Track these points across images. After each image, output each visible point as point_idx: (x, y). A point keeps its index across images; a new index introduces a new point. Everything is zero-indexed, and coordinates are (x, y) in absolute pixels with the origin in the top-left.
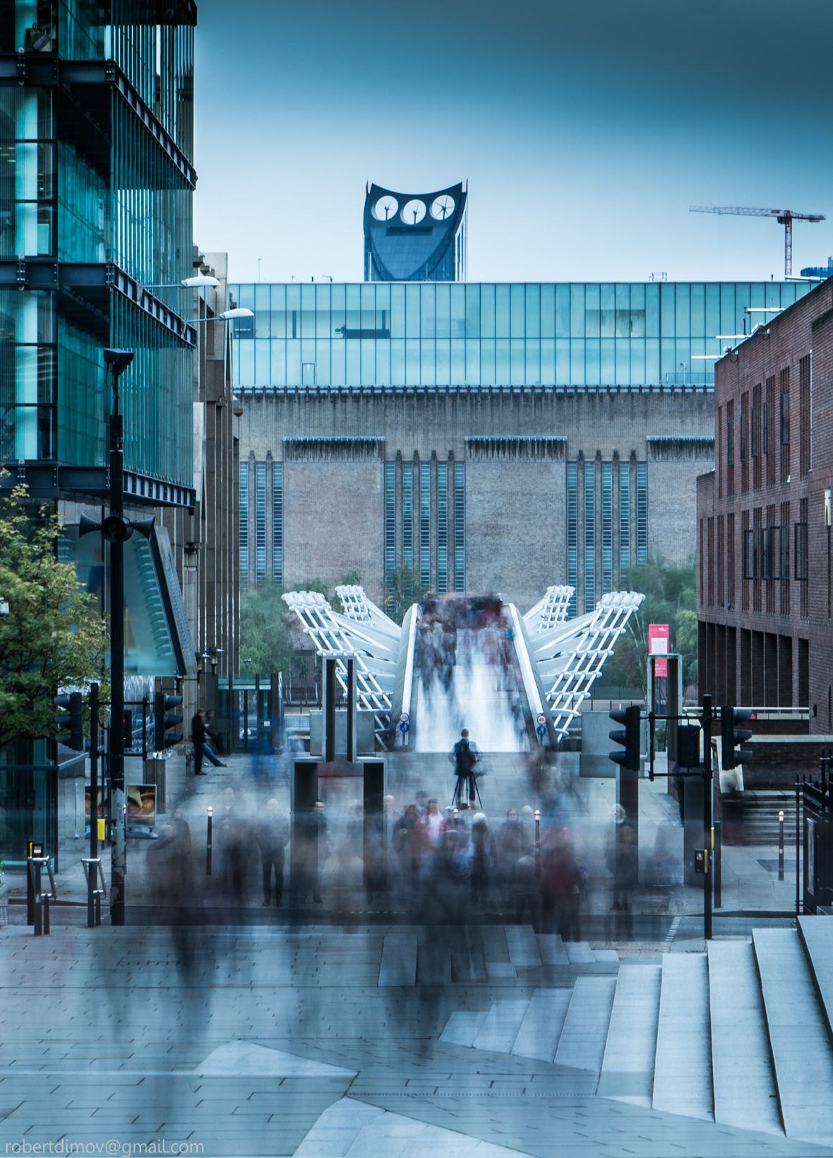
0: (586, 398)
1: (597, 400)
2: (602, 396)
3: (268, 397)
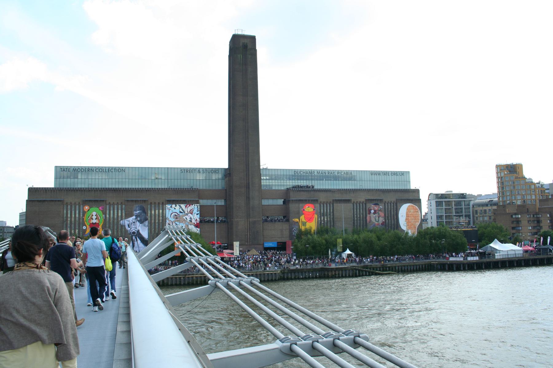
0: (152, 191)
2: (156, 190)
3: (79, 190)
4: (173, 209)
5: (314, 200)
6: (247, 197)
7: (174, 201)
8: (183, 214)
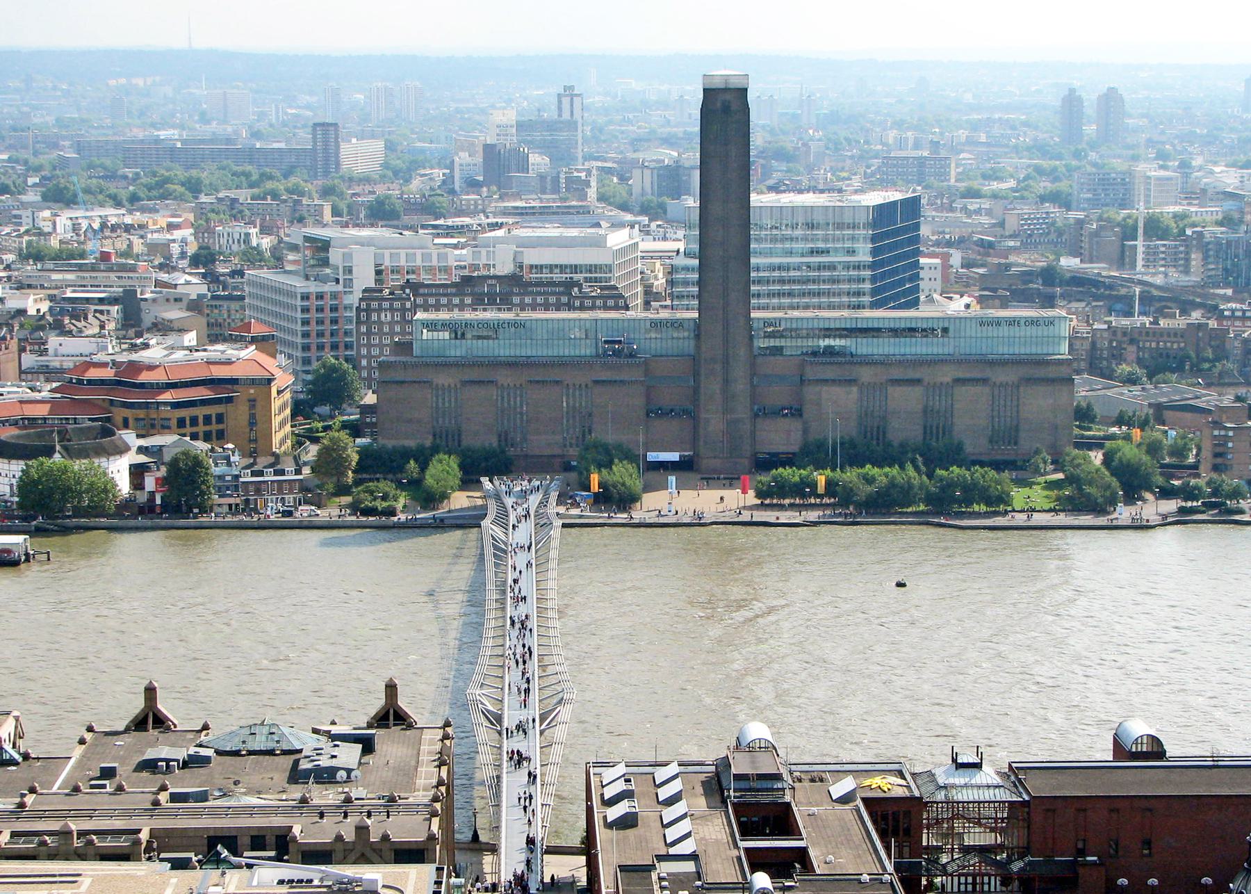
5: (850, 381)
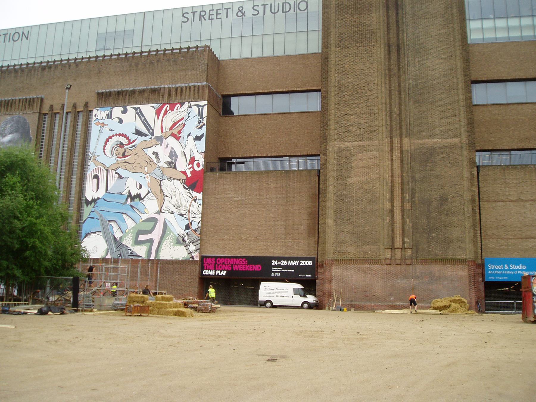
1: (67, 68)
4: (113, 123)
6: (389, 46)
7: (119, 93)
8: (148, 138)
